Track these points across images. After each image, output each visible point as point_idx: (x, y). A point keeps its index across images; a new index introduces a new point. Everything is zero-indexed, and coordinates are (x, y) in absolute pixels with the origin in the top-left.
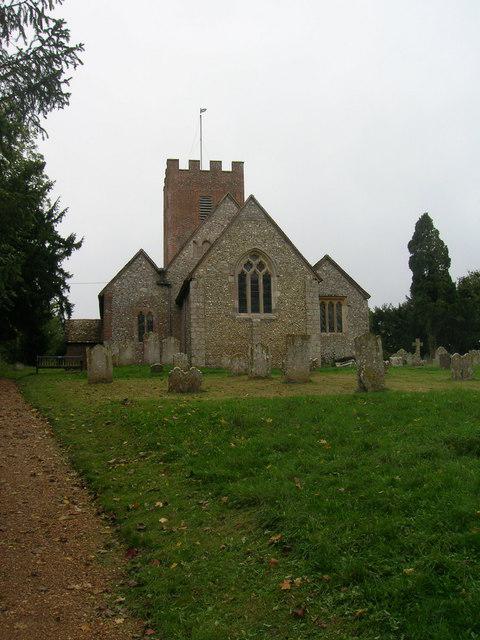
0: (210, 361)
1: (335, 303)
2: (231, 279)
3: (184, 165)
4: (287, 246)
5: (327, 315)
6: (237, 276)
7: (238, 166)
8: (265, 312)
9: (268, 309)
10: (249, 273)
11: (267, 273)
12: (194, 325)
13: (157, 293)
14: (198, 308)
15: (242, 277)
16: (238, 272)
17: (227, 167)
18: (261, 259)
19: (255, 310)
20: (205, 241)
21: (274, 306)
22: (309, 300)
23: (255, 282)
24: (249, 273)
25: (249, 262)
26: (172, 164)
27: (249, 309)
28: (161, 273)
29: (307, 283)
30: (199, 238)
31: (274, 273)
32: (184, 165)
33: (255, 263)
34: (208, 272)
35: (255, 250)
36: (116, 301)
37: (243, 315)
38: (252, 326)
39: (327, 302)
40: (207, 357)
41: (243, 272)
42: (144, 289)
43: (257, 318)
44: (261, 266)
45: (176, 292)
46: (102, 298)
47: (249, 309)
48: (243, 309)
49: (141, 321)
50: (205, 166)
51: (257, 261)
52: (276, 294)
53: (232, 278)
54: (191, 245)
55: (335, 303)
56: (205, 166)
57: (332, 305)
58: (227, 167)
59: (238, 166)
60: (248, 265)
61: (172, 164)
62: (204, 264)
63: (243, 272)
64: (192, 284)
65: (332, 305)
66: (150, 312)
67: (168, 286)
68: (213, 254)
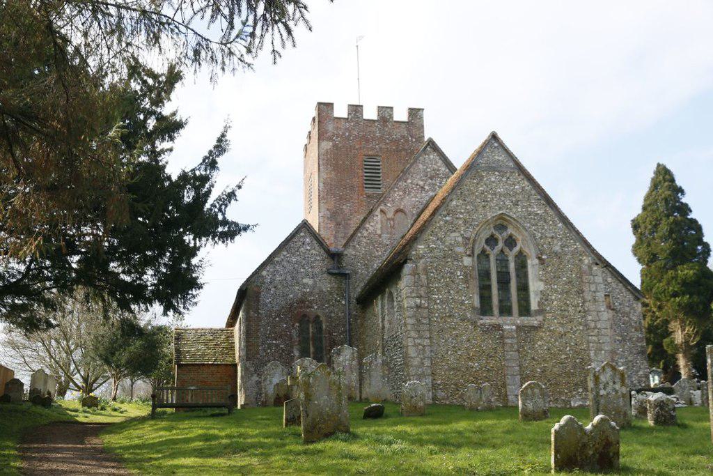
0: (440, 394)
2: (467, 261)
3: (341, 111)
4: (551, 212)
6: (476, 255)
7: (415, 113)
8: (521, 314)
9: (525, 310)
10: (493, 254)
11: (520, 253)
13: (327, 284)
14: (418, 307)
16: (477, 252)
17: (401, 115)
18: (510, 231)
19: (505, 310)
20: (398, 211)
21: (534, 306)
22: (588, 297)
23: (502, 261)
24: (493, 254)
25: (492, 236)
26: (324, 109)
27: (496, 311)
28: (335, 257)
29: (585, 267)
30: (390, 208)
31: (531, 252)
32: (341, 111)
33: (501, 238)
34: (431, 250)
35: (501, 217)
36: (266, 299)
37: (487, 320)
38: (502, 337)
40: (434, 387)
41: (483, 251)
42: (309, 281)
43: (510, 324)
44: (511, 242)
45: (358, 288)
46: (243, 294)
47: (496, 311)
48: (485, 309)
49: (303, 332)
50: (370, 113)
51: (505, 234)
52: (535, 286)
54: (378, 216)
56: (370, 113)
58: (401, 115)
59: (415, 113)
60: (492, 241)
61: (324, 109)
62: (426, 236)
64: (408, 268)
66: (318, 317)
67: (345, 276)
68: (440, 221)
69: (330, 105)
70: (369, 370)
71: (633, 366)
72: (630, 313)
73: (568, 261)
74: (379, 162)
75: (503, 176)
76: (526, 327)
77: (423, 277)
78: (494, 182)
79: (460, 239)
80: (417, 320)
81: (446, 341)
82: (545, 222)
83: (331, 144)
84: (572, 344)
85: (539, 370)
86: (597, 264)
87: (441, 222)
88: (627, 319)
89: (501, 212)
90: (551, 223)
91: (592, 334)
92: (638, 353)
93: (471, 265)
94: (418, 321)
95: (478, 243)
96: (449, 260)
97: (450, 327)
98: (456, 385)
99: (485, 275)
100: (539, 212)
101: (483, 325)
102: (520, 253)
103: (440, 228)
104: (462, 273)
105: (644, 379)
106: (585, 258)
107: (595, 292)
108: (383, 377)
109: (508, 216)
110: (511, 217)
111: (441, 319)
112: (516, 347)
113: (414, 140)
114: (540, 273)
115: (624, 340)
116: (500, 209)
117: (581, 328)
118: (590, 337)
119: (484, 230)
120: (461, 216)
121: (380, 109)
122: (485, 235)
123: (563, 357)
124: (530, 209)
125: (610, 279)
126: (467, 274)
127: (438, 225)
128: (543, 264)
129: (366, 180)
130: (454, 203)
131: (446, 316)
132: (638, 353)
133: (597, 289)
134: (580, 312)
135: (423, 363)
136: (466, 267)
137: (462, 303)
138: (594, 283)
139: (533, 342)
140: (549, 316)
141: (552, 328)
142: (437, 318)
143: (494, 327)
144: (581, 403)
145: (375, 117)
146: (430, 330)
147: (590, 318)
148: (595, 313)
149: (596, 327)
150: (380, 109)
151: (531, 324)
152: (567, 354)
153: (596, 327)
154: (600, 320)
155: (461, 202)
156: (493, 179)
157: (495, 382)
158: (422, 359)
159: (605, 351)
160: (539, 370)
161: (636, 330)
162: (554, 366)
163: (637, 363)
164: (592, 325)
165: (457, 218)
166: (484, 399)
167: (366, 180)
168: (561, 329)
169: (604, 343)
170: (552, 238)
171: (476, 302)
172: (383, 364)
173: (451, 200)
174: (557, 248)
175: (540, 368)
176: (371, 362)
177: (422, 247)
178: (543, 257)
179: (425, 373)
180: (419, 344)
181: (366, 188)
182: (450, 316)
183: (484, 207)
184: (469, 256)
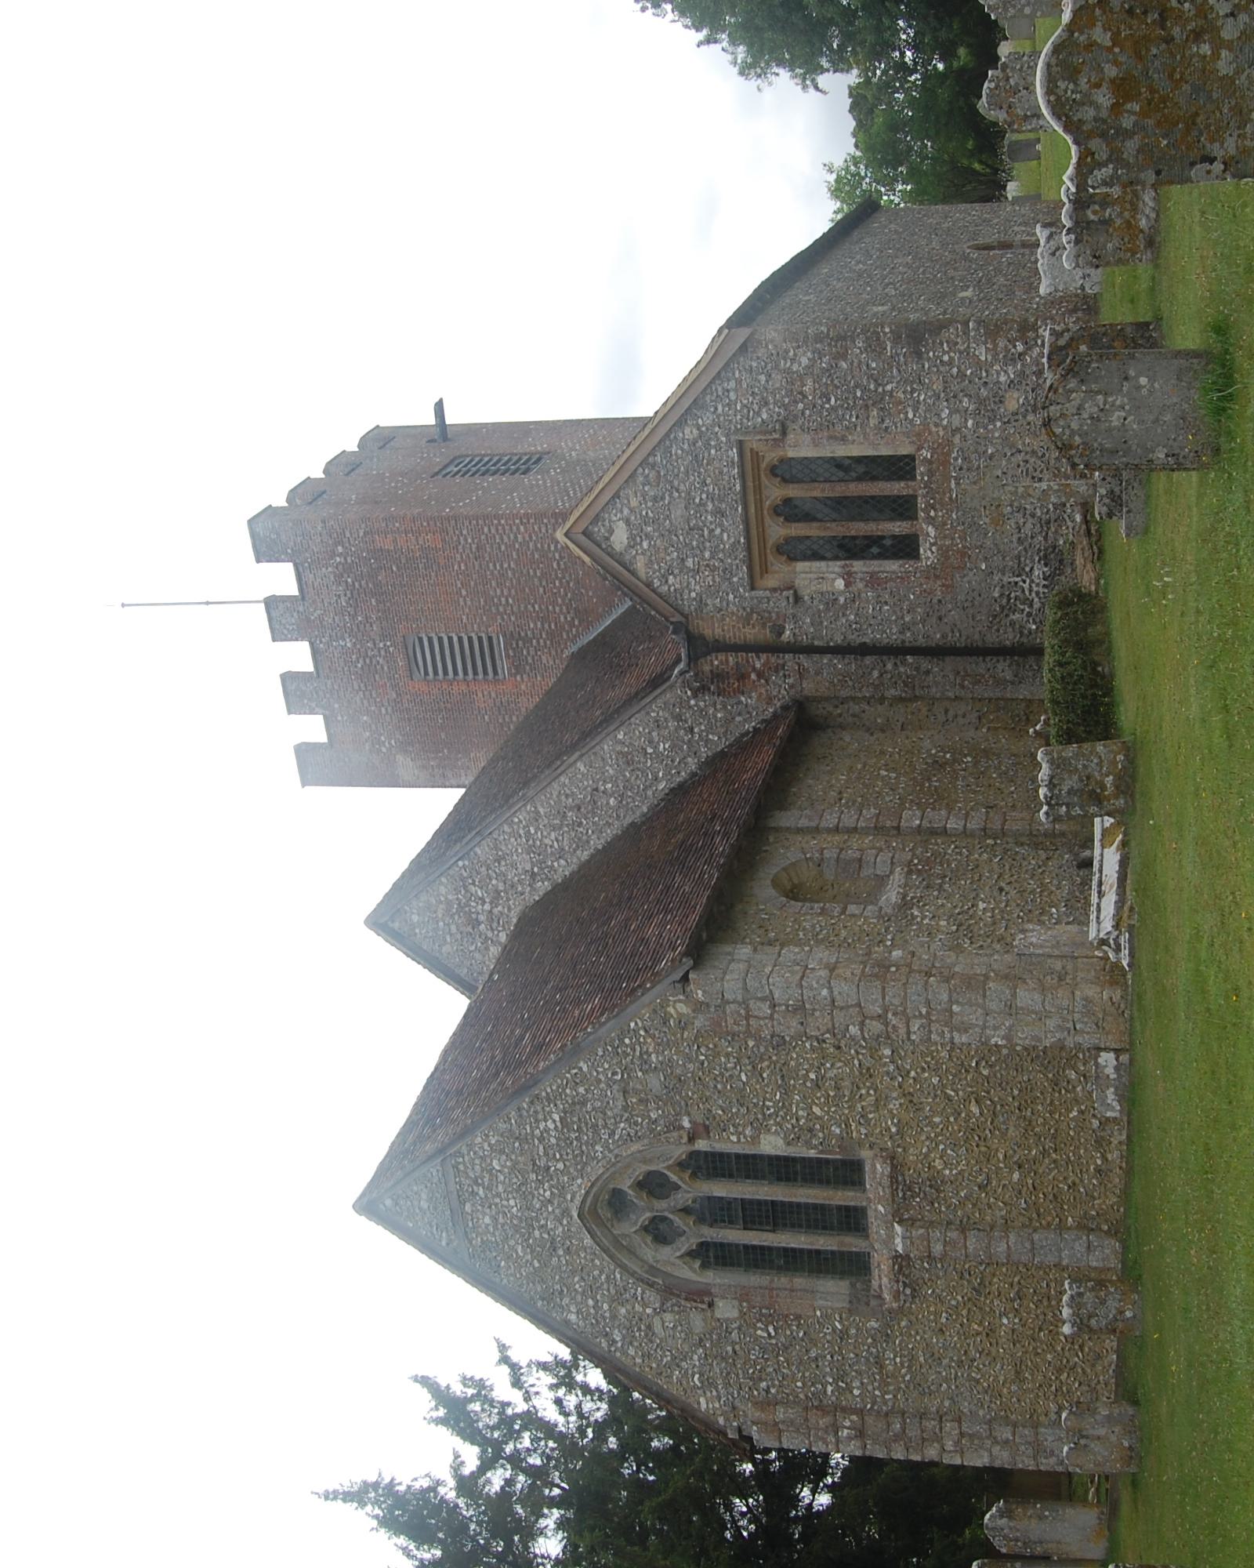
1: (775, 492)
2: (726, 1310)
5: (837, 529)
12: (932, 1453)
15: (714, 1255)
16: (690, 1273)
18: (626, 1185)
19: (853, 1220)
23: (718, 1212)
32: (313, 728)
37: (882, 1277)
39: (777, 531)
44: (653, 1185)
53: (720, 1304)
55: (775, 492)
56: (299, 656)
57: (788, 511)
58: (282, 579)
63: (691, 1254)
65: (788, 511)
69: (305, 753)
70: (1025, 1543)
71: (961, 375)
72: (788, 371)
73: (689, 1059)
74: (420, 640)
75: (474, 1194)
76: (893, 1194)
77: (781, 1414)
78: (495, 1219)
79: (668, 1317)
80: (895, 1441)
81: (947, 1380)
82: (583, 1103)
83: (400, 758)
84: (935, 1080)
85: (1016, 1176)
86: (685, 979)
87: (632, 1352)
88: (809, 382)
89: (575, 1214)
90: (581, 1090)
91: (902, 1031)
92: (919, 355)
93: (736, 1302)
94: (897, 1438)
95: (669, 1269)
96: (729, 1349)
97: (910, 1367)
98: (1060, 1371)
99: (757, 1258)
100: (556, 1117)
101: (897, 1295)
102: (681, 1165)
103: (647, 1356)
104: (759, 1325)
105: (1002, 343)
106: (671, 1010)
107: (773, 1006)
108: (1041, 1518)
109: (583, 1202)
110: (587, 1193)
111: (889, 1384)
112: (953, 1235)
113: (340, 549)
114: (734, 1138)
115: (879, 400)
116: (566, 1212)
117: (887, 1052)
118: (913, 1037)
119: (631, 1252)
120: (606, 1306)
121: (279, 633)
122: (650, 1252)
123: (975, 1109)
124: (553, 1141)
125: (687, 431)
126: (761, 1315)
127: (639, 1361)
128: (707, 1129)
129: (475, 673)
130: (573, 1317)
131: (881, 1373)
132: (919, 355)
133: (763, 999)
134: (839, 1048)
135: (1007, 1442)
136: (742, 1314)
137: (843, 1335)
138: (744, 1003)
139: (936, 1183)
140: (859, 1132)
141: (894, 1130)
142: (886, 1393)
143: (901, 1268)
144: (1110, 1094)
145: (304, 647)
146: (922, 1416)
147: (854, 1030)
148: (840, 1018)
149: (881, 1018)
150: (279, 633)
151: (886, 1182)
152: (966, 1101)
153: (881, 1018)
154: (859, 1005)
155: (566, 1301)
156: (487, 1220)
157: (1053, 1285)
158: (996, 1442)
159: (951, 1002)
160: (1016, 1176)
161: (843, 356)
162: (1004, 1134)
163: (951, 362)
164: (876, 1027)
165: (614, 1317)
166: (1102, 1432)
167: (475, 673)
168: (894, 1105)
169: (928, 1003)
170: (625, 1092)
171: (833, 1291)
172: (1010, 1518)
173: (567, 1322)
174: (655, 1082)
175: (1011, 1172)
176: (1005, 1537)
177: (702, 1400)
178: (686, 1124)
179: (1029, 1439)
180: (957, 1443)
181: (495, 672)
182: (882, 1367)
183: (568, 1251)
184: (711, 1305)
